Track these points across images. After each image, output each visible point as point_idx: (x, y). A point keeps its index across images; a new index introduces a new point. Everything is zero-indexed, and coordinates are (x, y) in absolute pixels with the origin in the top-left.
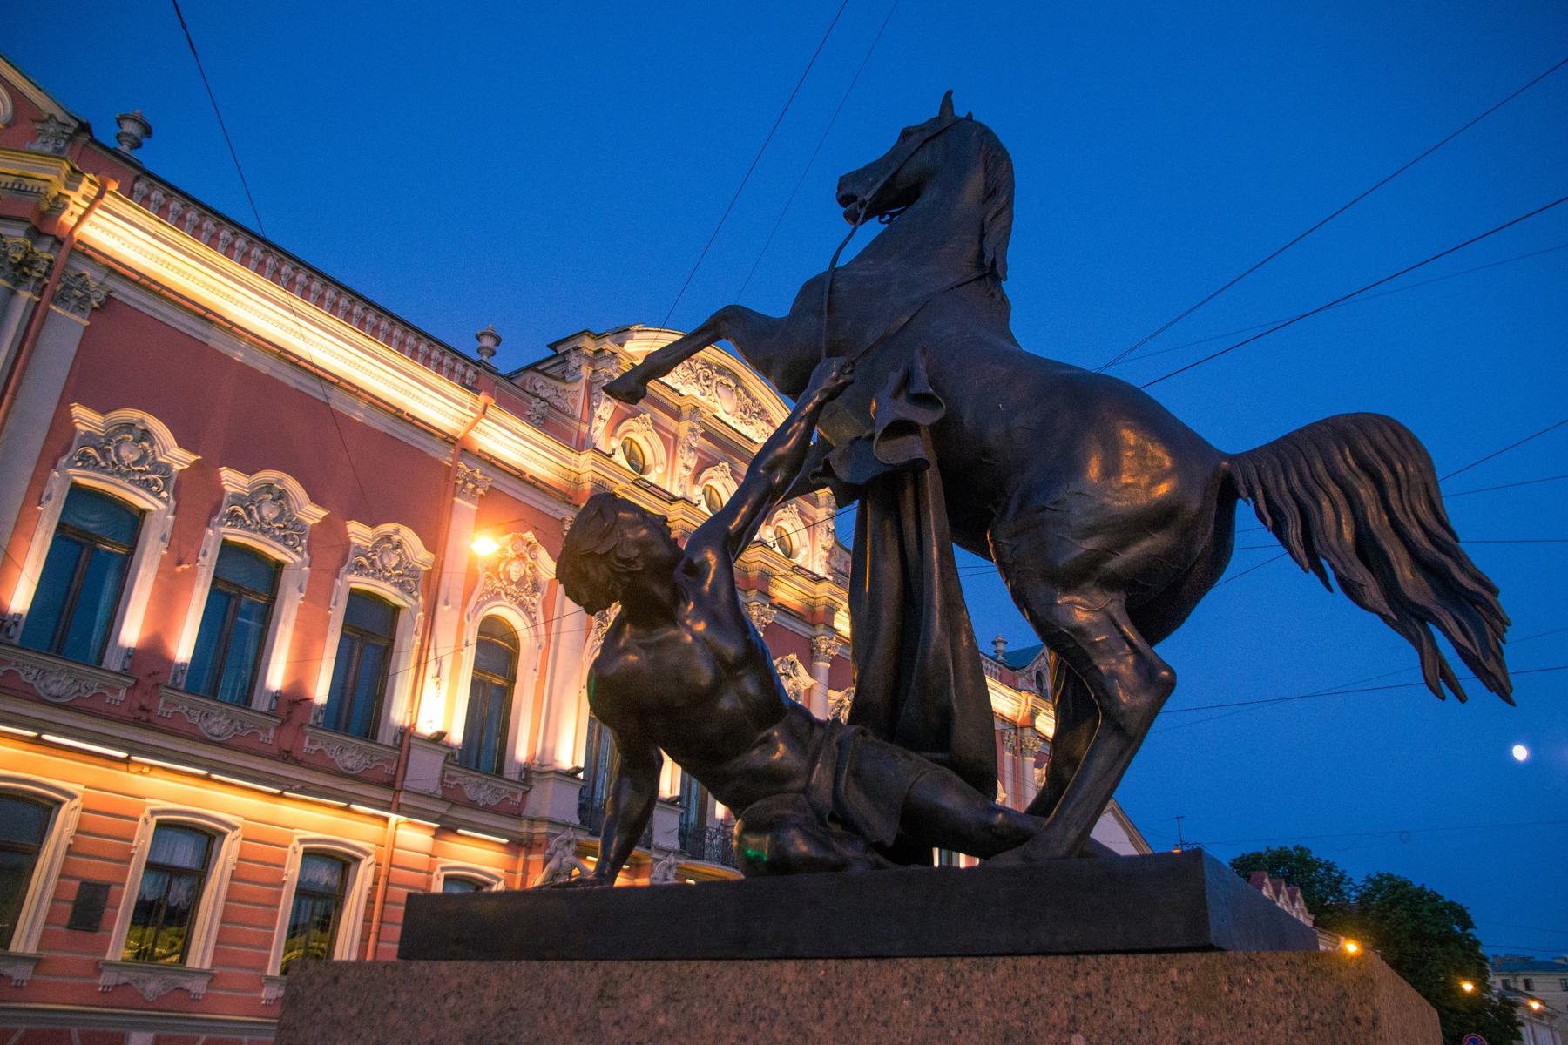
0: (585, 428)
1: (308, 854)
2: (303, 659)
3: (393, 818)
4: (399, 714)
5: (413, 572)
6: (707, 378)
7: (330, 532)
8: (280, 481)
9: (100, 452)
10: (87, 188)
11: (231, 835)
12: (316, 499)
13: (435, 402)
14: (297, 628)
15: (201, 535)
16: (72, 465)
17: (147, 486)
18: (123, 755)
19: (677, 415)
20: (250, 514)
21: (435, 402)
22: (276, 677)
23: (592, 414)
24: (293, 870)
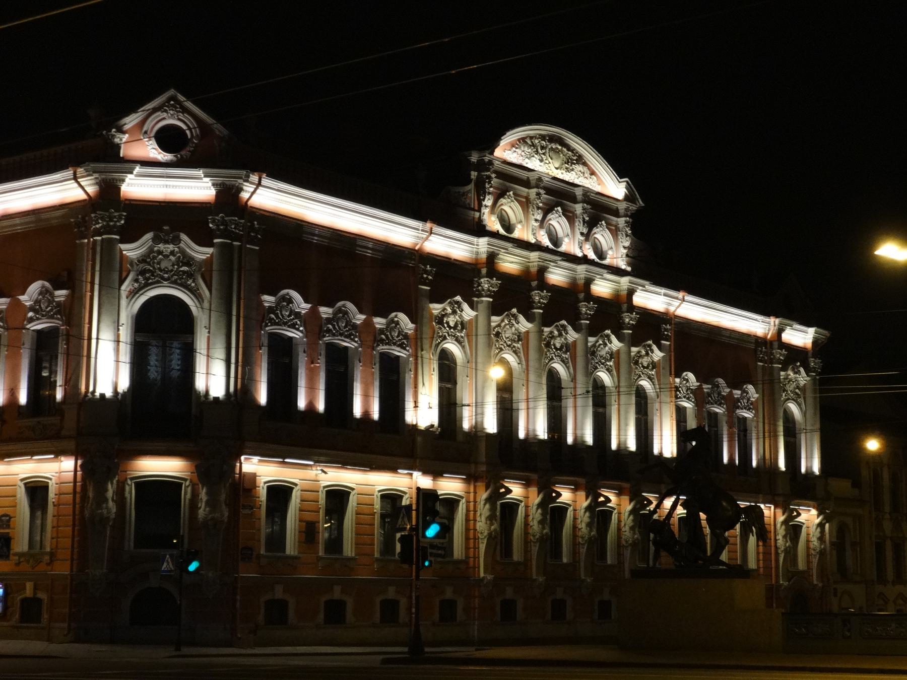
0: (477, 214)
1: (383, 497)
2: (366, 397)
6: (543, 148)
11: (353, 493)
16: (267, 326)
17: (293, 326)
18: (311, 463)
19: (527, 184)
23: (480, 205)
24: (377, 506)
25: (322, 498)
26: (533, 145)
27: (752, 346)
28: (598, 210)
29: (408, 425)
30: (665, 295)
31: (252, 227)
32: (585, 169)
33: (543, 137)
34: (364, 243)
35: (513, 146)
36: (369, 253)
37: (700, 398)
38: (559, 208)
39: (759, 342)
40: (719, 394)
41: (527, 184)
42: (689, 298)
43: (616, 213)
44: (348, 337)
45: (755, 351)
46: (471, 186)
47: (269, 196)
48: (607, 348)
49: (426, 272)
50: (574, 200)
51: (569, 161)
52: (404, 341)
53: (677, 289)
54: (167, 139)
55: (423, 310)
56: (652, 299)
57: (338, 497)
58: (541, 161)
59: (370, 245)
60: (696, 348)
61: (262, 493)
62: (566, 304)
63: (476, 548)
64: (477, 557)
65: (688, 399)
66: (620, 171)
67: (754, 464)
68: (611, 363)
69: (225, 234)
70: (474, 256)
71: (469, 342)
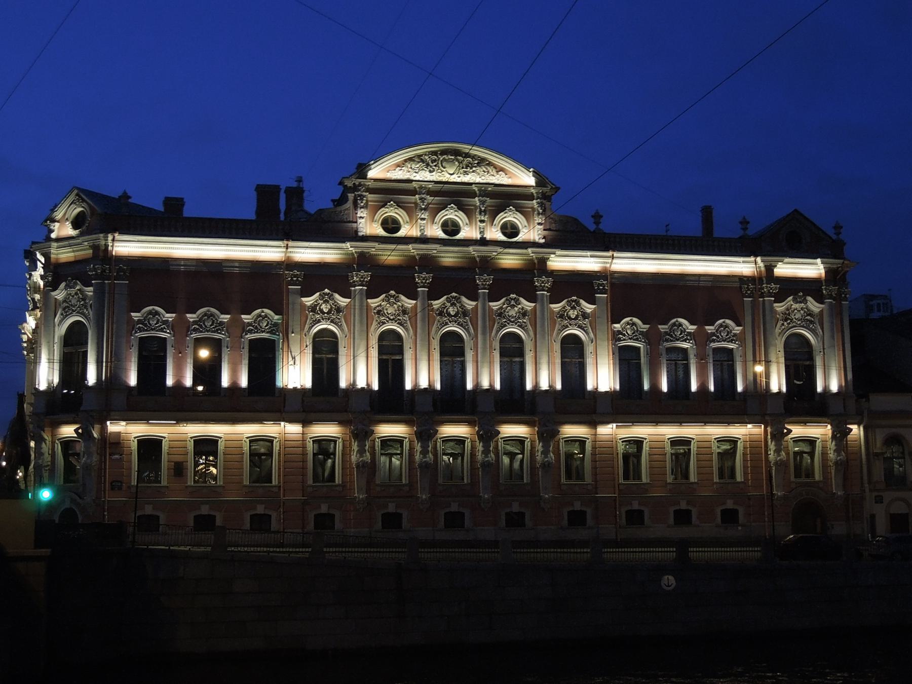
2: (234, 373)
4: (280, 383)
5: (276, 325)
6: (433, 161)
7: (236, 321)
8: (208, 311)
9: (144, 324)
10: (110, 237)
13: (268, 252)
15: (185, 340)
16: (136, 332)
17: (162, 330)
19: (413, 192)
20: (201, 326)
21: (268, 252)
22: (225, 382)
24: (246, 448)
25: (191, 446)
28: (504, 198)
31: (120, 270)
33: (434, 153)
35: (399, 166)
36: (237, 270)
37: (652, 339)
39: (742, 279)
41: (413, 192)
42: (616, 254)
43: (530, 197)
45: (741, 288)
46: (349, 204)
50: (473, 195)
52: (274, 328)
53: (607, 250)
54: (77, 223)
55: (294, 304)
56: (563, 262)
57: (206, 446)
58: (430, 172)
59: (237, 264)
60: (629, 295)
61: (134, 446)
63: (352, 474)
64: (352, 482)
65: (637, 339)
66: (525, 162)
67: (740, 388)
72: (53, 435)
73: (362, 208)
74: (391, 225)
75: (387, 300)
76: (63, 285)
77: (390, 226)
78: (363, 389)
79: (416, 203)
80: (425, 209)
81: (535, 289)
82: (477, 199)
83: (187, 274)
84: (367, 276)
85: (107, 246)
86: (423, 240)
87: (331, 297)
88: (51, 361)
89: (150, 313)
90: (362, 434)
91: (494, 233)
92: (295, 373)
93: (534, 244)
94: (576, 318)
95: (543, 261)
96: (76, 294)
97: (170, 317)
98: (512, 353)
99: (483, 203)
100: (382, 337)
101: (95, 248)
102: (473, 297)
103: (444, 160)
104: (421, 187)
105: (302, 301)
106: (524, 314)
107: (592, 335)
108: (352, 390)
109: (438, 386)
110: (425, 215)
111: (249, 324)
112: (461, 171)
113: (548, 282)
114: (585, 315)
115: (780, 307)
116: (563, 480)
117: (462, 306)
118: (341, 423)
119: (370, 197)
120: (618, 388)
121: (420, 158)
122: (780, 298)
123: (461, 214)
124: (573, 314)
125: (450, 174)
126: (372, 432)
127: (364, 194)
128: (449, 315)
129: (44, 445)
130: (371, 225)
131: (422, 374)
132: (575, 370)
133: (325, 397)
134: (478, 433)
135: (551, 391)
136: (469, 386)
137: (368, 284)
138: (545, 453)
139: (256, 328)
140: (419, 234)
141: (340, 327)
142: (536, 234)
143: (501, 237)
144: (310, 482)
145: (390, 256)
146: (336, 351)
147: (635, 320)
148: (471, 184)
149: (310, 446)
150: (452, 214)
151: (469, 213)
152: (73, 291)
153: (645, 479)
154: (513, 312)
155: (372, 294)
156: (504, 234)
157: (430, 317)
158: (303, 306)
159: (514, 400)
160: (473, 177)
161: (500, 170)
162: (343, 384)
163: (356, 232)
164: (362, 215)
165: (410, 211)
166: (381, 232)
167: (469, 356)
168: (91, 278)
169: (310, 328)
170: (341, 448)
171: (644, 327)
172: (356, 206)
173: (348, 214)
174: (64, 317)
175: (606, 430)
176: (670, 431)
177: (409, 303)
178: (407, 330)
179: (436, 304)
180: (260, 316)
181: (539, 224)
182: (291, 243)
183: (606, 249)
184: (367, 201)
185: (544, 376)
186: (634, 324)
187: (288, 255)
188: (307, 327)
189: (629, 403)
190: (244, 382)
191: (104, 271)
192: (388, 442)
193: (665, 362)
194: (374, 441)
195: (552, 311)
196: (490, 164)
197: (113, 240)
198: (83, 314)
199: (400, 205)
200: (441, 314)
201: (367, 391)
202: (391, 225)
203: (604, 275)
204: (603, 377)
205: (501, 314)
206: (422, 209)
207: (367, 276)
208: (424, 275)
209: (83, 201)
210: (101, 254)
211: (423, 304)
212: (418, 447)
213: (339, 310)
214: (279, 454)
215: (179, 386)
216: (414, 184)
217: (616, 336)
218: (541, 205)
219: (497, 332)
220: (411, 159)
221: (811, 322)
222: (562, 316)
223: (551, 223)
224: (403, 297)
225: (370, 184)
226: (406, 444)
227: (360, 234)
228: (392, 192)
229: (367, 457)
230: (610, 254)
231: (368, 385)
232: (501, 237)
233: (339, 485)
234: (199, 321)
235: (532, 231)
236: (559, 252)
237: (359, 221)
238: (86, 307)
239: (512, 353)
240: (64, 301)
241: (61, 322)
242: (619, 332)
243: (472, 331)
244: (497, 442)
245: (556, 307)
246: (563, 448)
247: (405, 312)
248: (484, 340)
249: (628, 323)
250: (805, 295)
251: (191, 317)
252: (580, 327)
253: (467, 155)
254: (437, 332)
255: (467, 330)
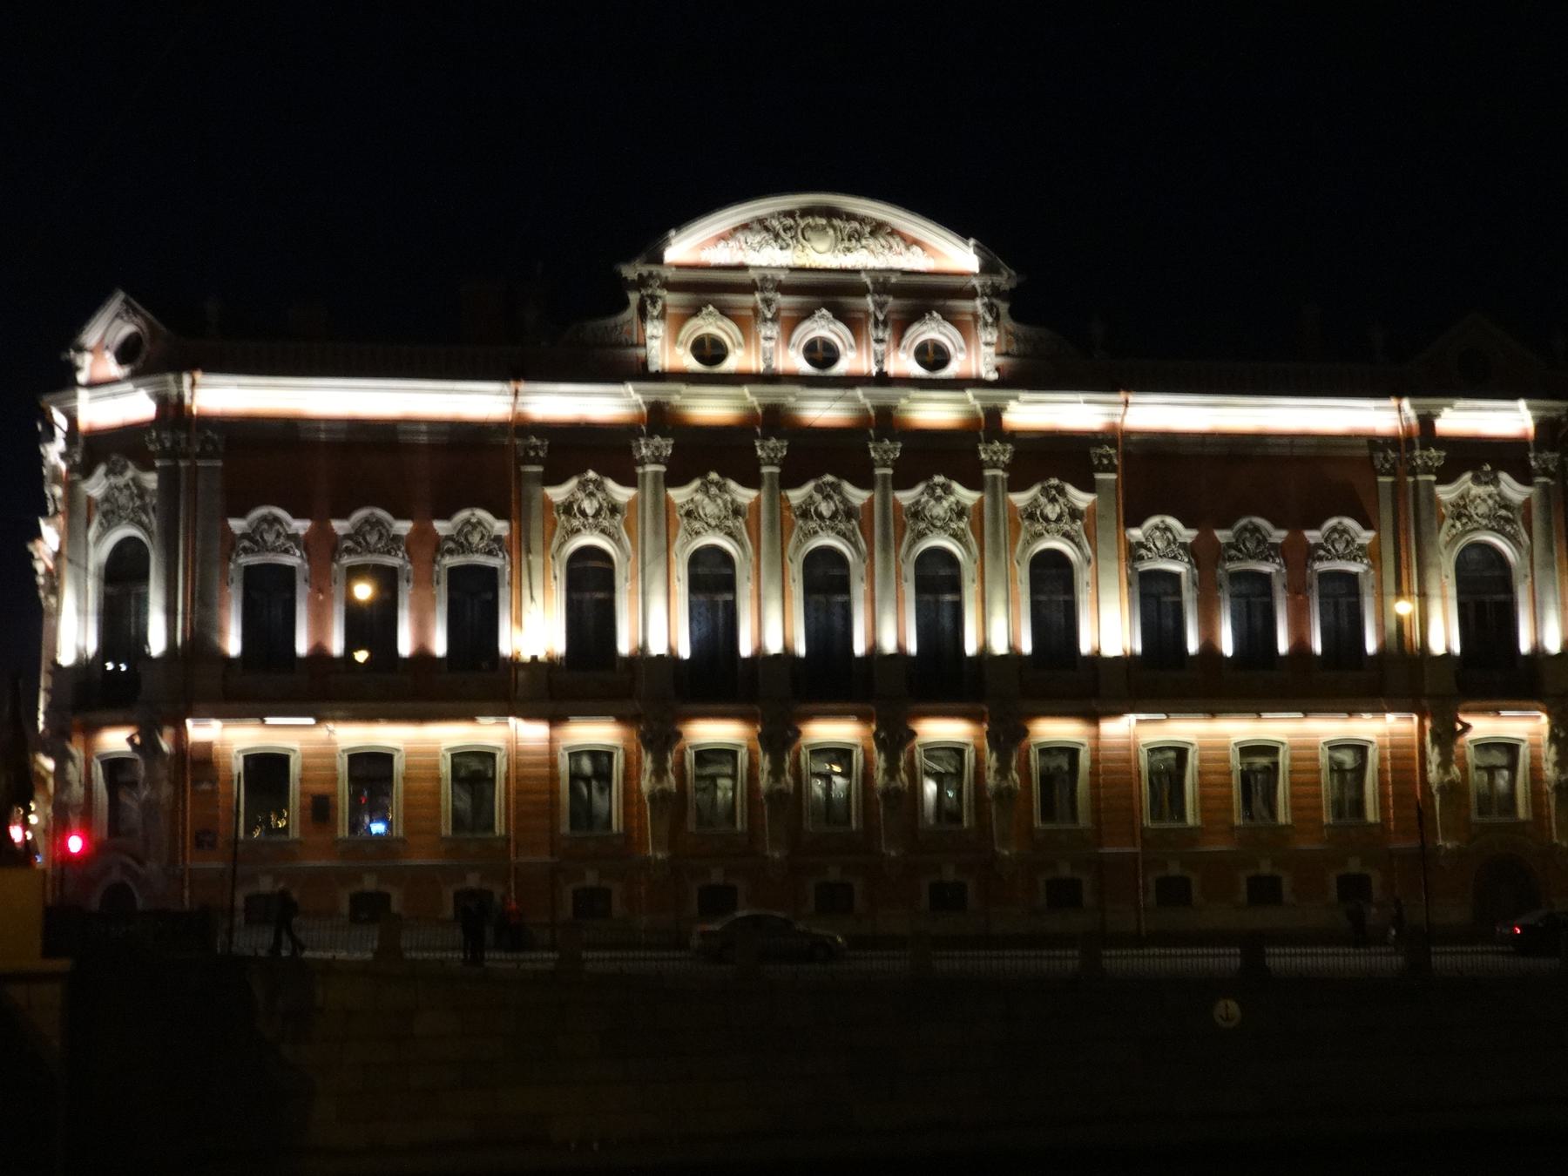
2: (422, 628)
3: (511, 720)
5: (498, 539)
7: (423, 534)
10: (186, 379)
12: (399, 516)
13: (480, 401)
14: (412, 608)
17: (286, 551)
19: (750, 288)
20: (359, 544)
21: (480, 401)
22: (405, 647)
25: (343, 766)
26: (767, 229)
27: (1366, 452)
28: (922, 296)
29: (505, 659)
30: (1086, 402)
31: (208, 440)
32: (895, 242)
33: (790, 214)
34: (409, 427)
36: (424, 439)
37: (1202, 555)
38: (824, 311)
39: (1375, 443)
40: (1262, 541)
41: (750, 288)
43: (971, 294)
44: (389, 553)
45: (1371, 458)
46: (632, 312)
47: (219, 396)
48: (952, 499)
49: (535, 448)
50: (862, 291)
51: (856, 236)
52: (497, 545)
54: (125, 354)
55: (529, 499)
56: (1031, 412)
59: (424, 428)
60: (1158, 475)
61: (238, 766)
62: (877, 451)
63: (641, 815)
65: (1175, 558)
66: (962, 229)
67: (1371, 646)
68: (962, 525)
69: (163, 454)
70: (636, 411)
71: (629, 531)
72: (89, 748)
73: (653, 318)
74: (709, 350)
75: (705, 489)
76: (101, 470)
77: (709, 351)
78: (660, 657)
79: (755, 310)
80: (773, 320)
81: (981, 465)
82: (869, 299)
83: (329, 445)
84: (666, 446)
85: (181, 397)
86: (771, 378)
87: (599, 486)
88: (82, 612)
89: (264, 519)
90: (660, 737)
91: (904, 363)
92: (535, 629)
93: (977, 383)
94: (1059, 519)
95: (994, 415)
96: (127, 486)
97: (301, 526)
98: (938, 585)
99: (880, 306)
100: (696, 559)
101: (162, 401)
102: (865, 482)
103: (808, 225)
104: (764, 279)
105: (545, 497)
106: (960, 512)
107: (1088, 551)
108: (641, 658)
109: (801, 649)
110: (771, 330)
111: (449, 538)
112: (840, 247)
113: (1004, 453)
114: (1075, 514)
115: (1446, 493)
116: (1037, 823)
117: (845, 501)
118: (621, 719)
119: (670, 298)
120: (1138, 648)
121: (762, 224)
122: (1447, 476)
123: (841, 328)
124: (1052, 511)
125: (821, 254)
126: (679, 735)
127: (659, 292)
128: (820, 516)
129: (70, 766)
130: (672, 351)
131: (771, 625)
132: (1058, 618)
133: (591, 670)
134: (876, 735)
135: (1014, 655)
136: (859, 648)
137: (669, 462)
138: (1003, 770)
139: (461, 545)
140: (762, 367)
141: (618, 542)
142: (981, 360)
143: (918, 371)
144: (565, 828)
145: (712, 408)
146: (610, 586)
147: (1172, 521)
148: (857, 271)
149: (564, 765)
150: (823, 328)
151: (854, 323)
152: (120, 481)
153: (1191, 819)
154: (939, 510)
155: (676, 477)
156: (922, 363)
157: (783, 523)
158: (548, 505)
159: (942, 673)
160: (866, 258)
161: (910, 242)
162: (624, 647)
163: (645, 364)
164: (655, 332)
165: (746, 323)
166: (691, 363)
167: (859, 591)
168: (153, 455)
169: (561, 545)
170: (621, 765)
171: (1188, 535)
172: (643, 314)
173: (630, 333)
174: (106, 528)
175: (1121, 729)
176: (1237, 730)
177: (745, 496)
178: (742, 545)
179: (796, 496)
180: (468, 522)
181: (987, 344)
182: (523, 387)
183: (1114, 388)
184: (664, 307)
185: (997, 626)
186: (1167, 529)
187: (519, 408)
188: (555, 543)
189: (1161, 676)
190: (439, 645)
191: (176, 443)
192: (710, 755)
193: (1227, 596)
194: (682, 753)
195: (1012, 508)
196: (894, 232)
197: (193, 384)
198: (141, 524)
199: (725, 311)
200: (805, 514)
201: (671, 660)
202: (709, 350)
203: (1111, 437)
204: (1109, 627)
205: (916, 513)
206: (765, 320)
207: (666, 446)
208: (773, 442)
209: (136, 312)
210: (171, 412)
211: (771, 498)
212: (765, 763)
213: (614, 509)
214: (507, 779)
215: (320, 652)
216: (753, 274)
217: (1134, 552)
218: (990, 308)
219: (910, 547)
220: (745, 227)
221: (1508, 520)
222: (1031, 516)
223: (1008, 342)
224: (732, 485)
225: (670, 274)
226: (743, 758)
227: (653, 368)
228: (710, 288)
229: (671, 781)
230: (1121, 397)
231: (670, 648)
232: (918, 371)
233: (618, 835)
234: (357, 532)
235: (977, 356)
236: (1025, 396)
237: (649, 342)
238: (144, 509)
239: (938, 585)
240: (107, 499)
241: (99, 538)
242: (1140, 545)
243: (863, 545)
244: (912, 752)
245: (1020, 499)
246: (1035, 761)
247: (737, 511)
248: (886, 560)
249: (1157, 528)
250: (1495, 470)
251: (340, 526)
252: (1067, 535)
253: (850, 217)
254: (797, 548)
255: (855, 545)
